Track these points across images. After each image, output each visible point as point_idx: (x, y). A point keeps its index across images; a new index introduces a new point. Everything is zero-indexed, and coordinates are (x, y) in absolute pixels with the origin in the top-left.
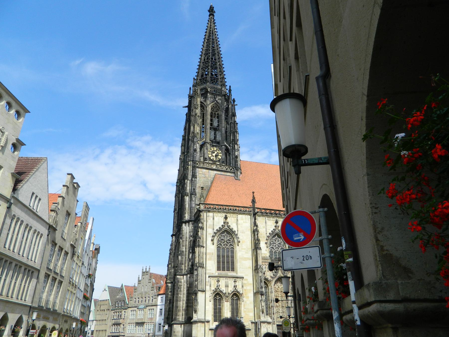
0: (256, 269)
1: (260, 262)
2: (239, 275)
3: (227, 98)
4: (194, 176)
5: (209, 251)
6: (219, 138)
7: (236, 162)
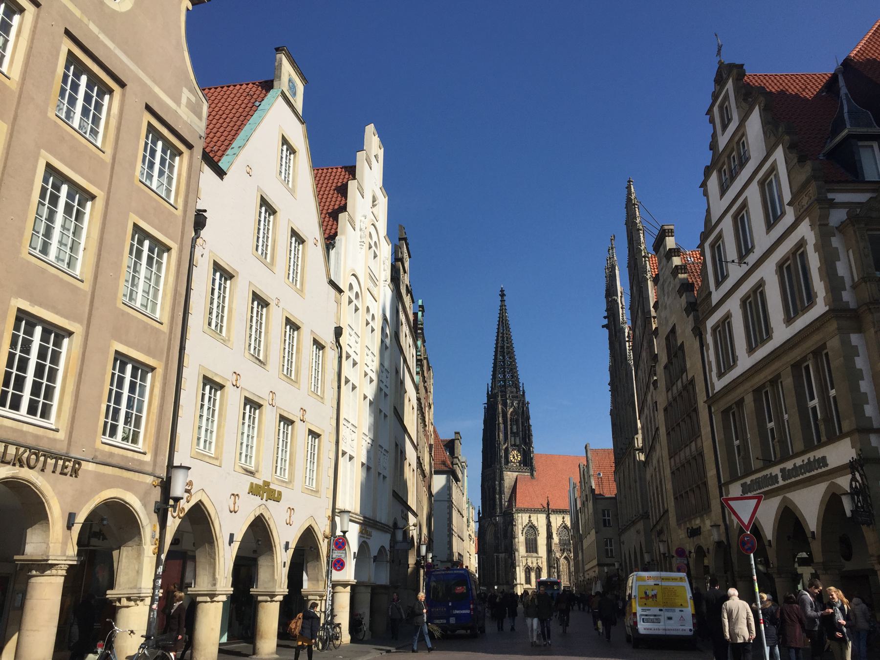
0: (549, 551)
1: (553, 548)
2: (540, 555)
3: (523, 403)
4: (502, 479)
5: (520, 540)
6: (518, 443)
7: (532, 463)
